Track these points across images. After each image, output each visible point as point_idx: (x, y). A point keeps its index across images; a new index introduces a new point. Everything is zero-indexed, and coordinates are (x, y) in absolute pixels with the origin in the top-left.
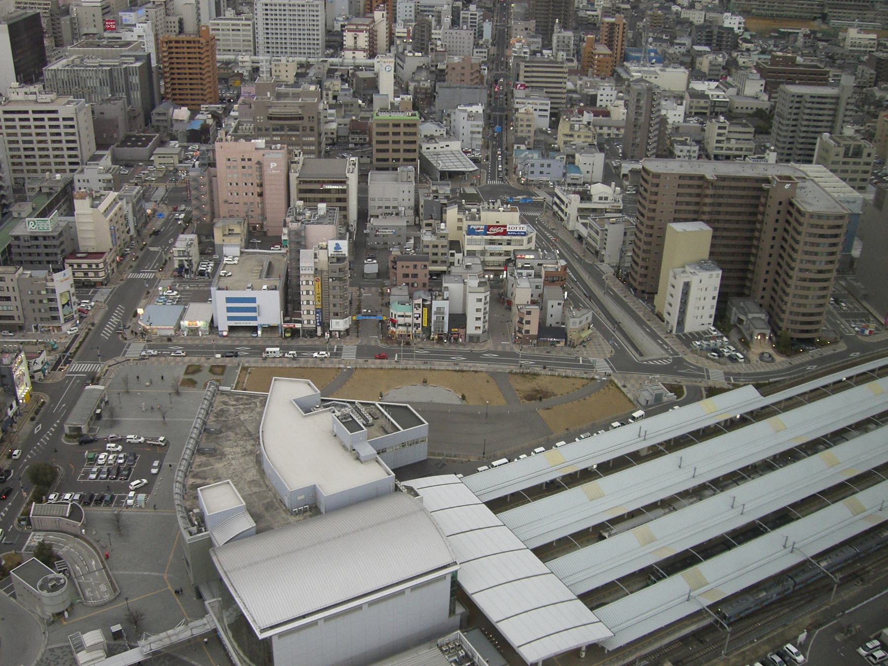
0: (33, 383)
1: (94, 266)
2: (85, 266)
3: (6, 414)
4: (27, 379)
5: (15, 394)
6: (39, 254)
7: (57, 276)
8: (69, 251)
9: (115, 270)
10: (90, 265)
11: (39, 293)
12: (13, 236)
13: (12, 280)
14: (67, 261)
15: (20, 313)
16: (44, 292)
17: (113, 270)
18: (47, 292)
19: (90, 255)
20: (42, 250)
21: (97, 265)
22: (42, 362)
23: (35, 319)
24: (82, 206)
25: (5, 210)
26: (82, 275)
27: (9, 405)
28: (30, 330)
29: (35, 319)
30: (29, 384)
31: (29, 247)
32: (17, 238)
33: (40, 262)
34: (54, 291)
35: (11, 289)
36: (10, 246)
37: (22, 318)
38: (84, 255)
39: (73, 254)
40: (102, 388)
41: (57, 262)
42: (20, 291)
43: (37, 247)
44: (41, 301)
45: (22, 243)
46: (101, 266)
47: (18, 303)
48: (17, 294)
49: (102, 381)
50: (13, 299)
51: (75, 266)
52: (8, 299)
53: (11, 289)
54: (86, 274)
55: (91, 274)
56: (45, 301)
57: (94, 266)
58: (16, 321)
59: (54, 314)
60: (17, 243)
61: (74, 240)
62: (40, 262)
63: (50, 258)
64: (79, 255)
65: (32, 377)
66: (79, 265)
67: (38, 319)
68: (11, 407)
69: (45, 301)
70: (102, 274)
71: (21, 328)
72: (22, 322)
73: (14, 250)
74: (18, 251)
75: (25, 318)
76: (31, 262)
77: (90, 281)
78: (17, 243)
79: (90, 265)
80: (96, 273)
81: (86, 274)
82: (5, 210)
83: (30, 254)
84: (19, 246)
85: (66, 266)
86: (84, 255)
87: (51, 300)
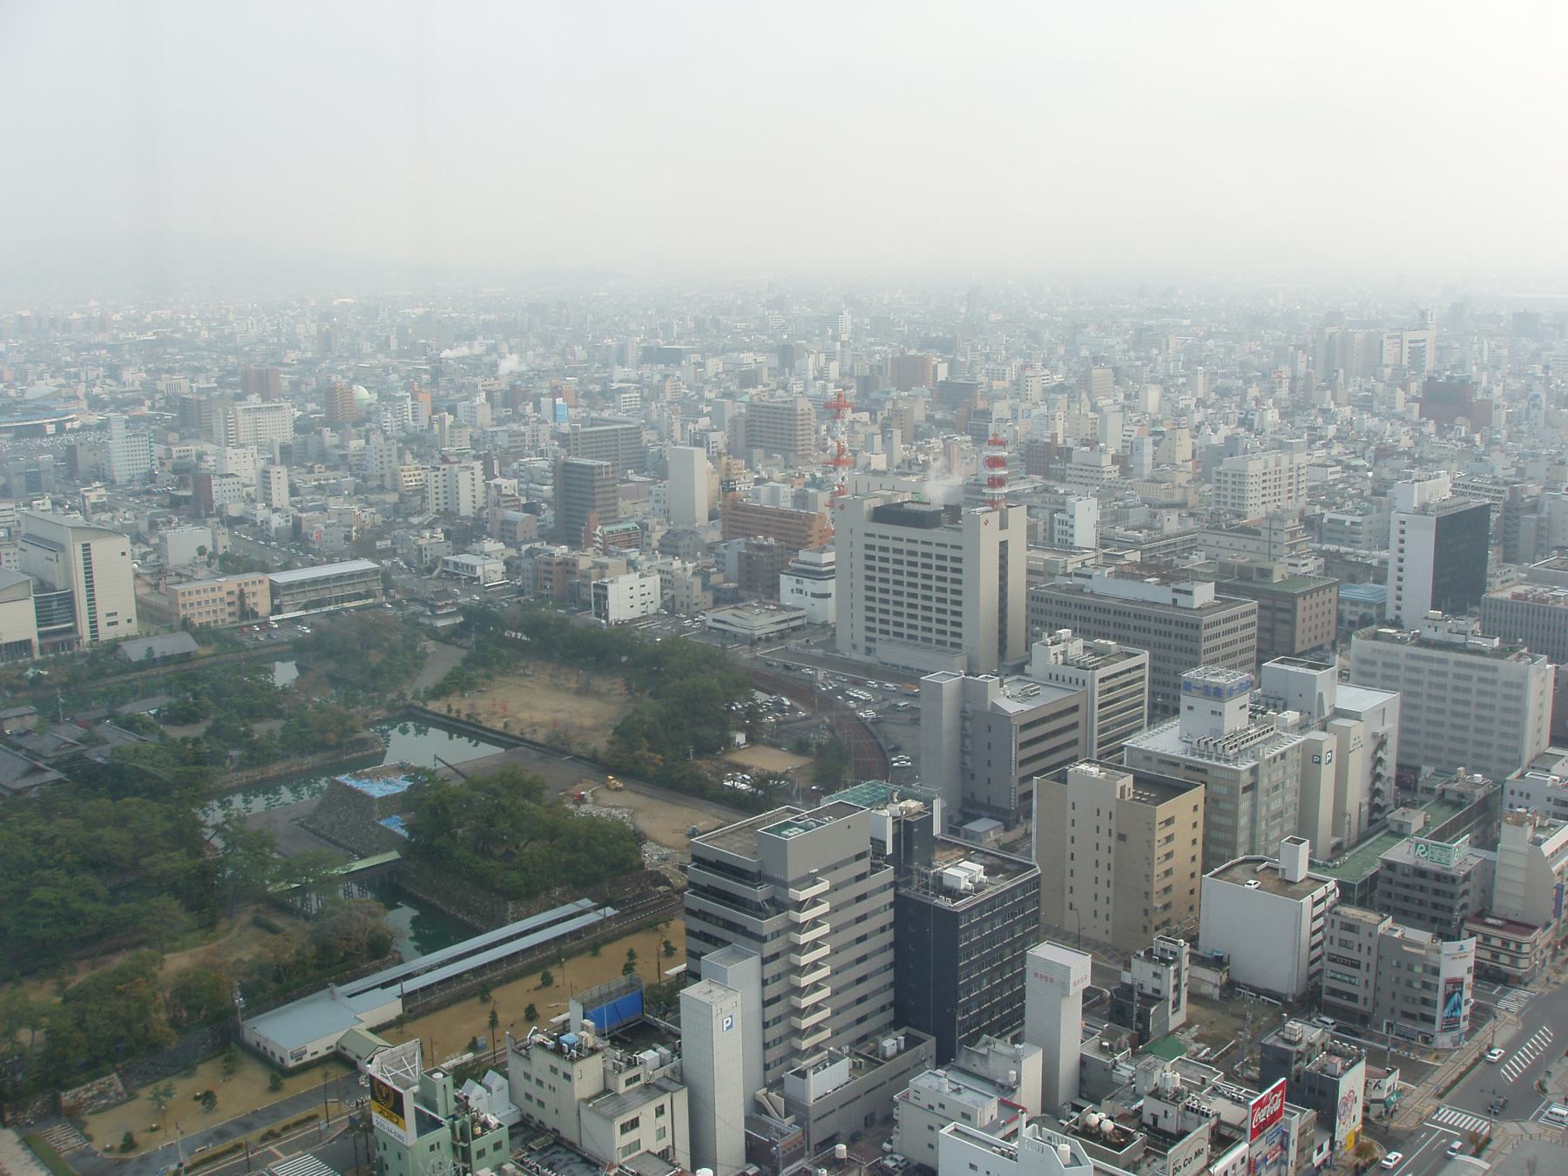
0: (1365, 1120)
1: (1512, 947)
2: (1496, 942)
3: (1310, 1159)
4: (1357, 1110)
5: (1332, 1129)
6: (1421, 903)
7: (1449, 947)
8: (1473, 908)
9: (1547, 963)
10: (1506, 943)
11: (1410, 968)
12: (1384, 861)
13: (1370, 935)
14: (1467, 925)
15: (1369, 993)
16: (1418, 969)
17: (1544, 960)
18: (1425, 971)
19: (1512, 924)
20: (1429, 898)
21: (1519, 945)
22: (1389, 1089)
23: (1392, 1011)
24: (1512, 838)
25: (1376, 815)
26: (1488, 955)
27: (1317, 1145)
28: (1379, 1027)
29: (1392, 1011)
30: (1359, 1119)
31: (1407, 886)
32: (1391, 866)
33: (1420, 916)
34: (1436, 972)
35: (1364, 949)
36: (1375, 876)
37: (1370, 1003)
38: (1500, 922)
39: (1480, 917)
40: (1486, 1166)
41: (1449, 923)
42: (1380, 957)
43: (1422, 889)
44: (1409, 984)
45: (1397, 877)
46: (1525, 949)
47: (1371, 976)
48: (1372, 959)
49: (1486, 1153)
50: (1363, 966)
51: (1480, 938)
52: (1356, 965)
53: (1364, 949)
54: (1495, 956)
55: (1504, 959)
56: (1417, 985)
57: (1512, 947)
58: (1359, 1006)
59: (1427, 1011)
60: (1390, 874)
61: (1487, 892)
62: (1420, 916)
63: (1437, 914)
64: (1490, 920)
65: (1366, 1109)
66: (1487, 938)
67: (1398, 1013)
68: (1320, 1149)
69: (1417, 985)
70: (1523, 963)
71: (1364, 1019)
72: (1368, 1008)
73: (1381, 885)
74: (1387, 887)
75: (1376, 1004)
76: (1405, 913)
77: (1498, 970)
78: (1390, 874)
79: (1506, 943)
80: (1514, 961)
81: (1495, 956)
82: (1376, 815)
83: (1406, 899)
84: (1390, 881)
85: (1464, 933)
86: (1500, 922)
87: (1426, 985)
